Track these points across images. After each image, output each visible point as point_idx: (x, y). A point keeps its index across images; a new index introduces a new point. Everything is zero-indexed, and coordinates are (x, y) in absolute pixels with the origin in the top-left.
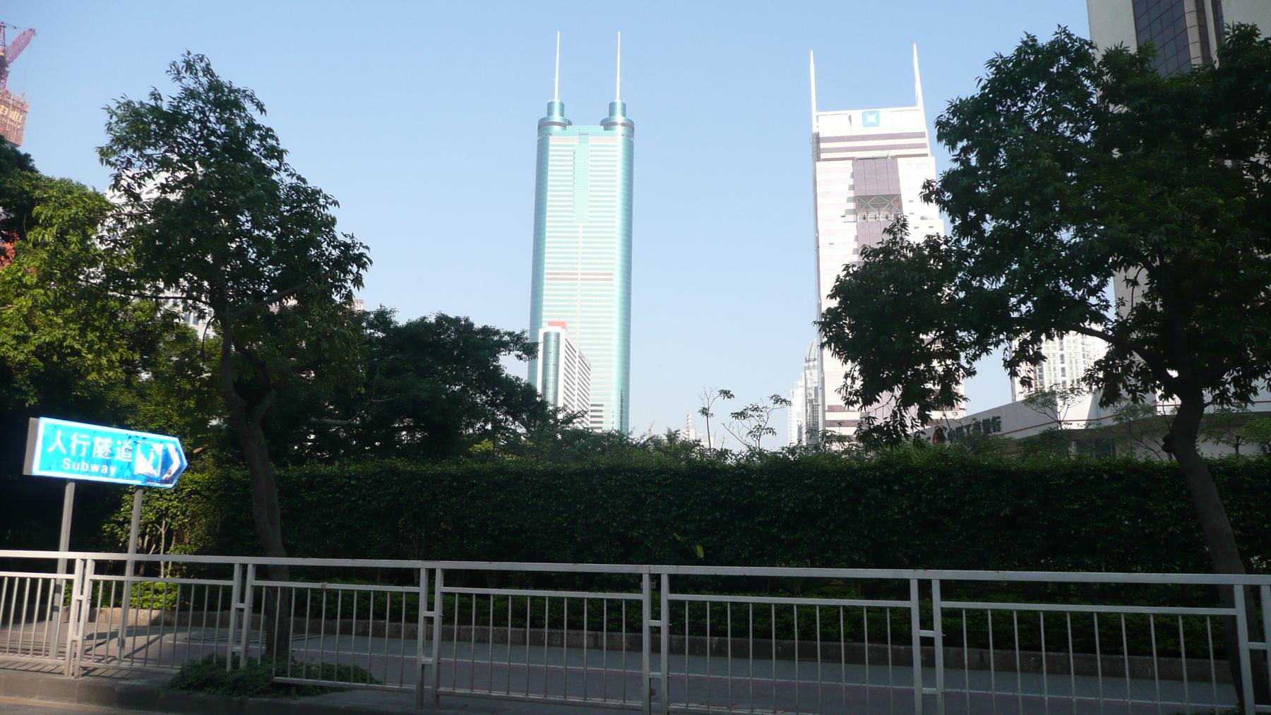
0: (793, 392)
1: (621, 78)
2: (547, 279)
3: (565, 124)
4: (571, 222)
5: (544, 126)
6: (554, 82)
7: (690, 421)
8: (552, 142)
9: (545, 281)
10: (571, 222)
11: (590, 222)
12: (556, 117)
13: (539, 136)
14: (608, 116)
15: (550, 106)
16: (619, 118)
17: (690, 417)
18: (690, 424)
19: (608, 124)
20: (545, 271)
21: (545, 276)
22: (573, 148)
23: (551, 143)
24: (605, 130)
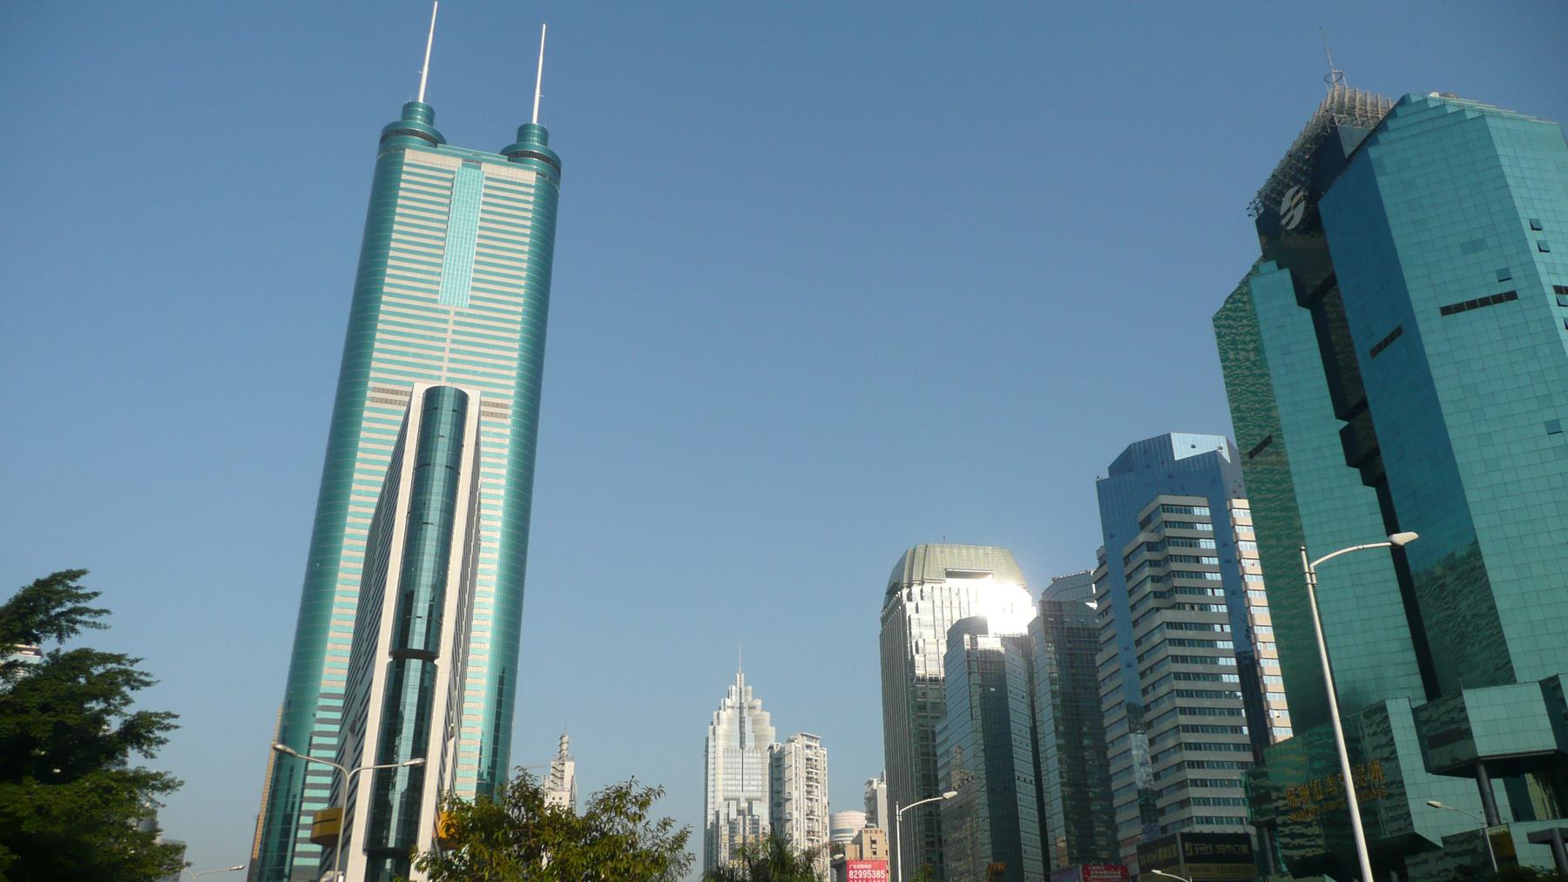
0: (718, 714)
1: (541, 94)
2: (373, 399)
3: (434, 140)
4: (435, 301)
5: (393, 138)
6: (421, 76)
7: (565, 746)
8: (410, 156)
9: (368, 404)
10: (435, 301)
11: (471, 306)
12: (419, 122)
14: (514, 141)
15: (409, 109)
16: (535, 144)
17: (565, 740)
18: (565, 752)
19: (515, 154)
20: (371, 384)
21: (369, 394)
22: (450, 176)
23: (406, 161)
24: (509, 160)
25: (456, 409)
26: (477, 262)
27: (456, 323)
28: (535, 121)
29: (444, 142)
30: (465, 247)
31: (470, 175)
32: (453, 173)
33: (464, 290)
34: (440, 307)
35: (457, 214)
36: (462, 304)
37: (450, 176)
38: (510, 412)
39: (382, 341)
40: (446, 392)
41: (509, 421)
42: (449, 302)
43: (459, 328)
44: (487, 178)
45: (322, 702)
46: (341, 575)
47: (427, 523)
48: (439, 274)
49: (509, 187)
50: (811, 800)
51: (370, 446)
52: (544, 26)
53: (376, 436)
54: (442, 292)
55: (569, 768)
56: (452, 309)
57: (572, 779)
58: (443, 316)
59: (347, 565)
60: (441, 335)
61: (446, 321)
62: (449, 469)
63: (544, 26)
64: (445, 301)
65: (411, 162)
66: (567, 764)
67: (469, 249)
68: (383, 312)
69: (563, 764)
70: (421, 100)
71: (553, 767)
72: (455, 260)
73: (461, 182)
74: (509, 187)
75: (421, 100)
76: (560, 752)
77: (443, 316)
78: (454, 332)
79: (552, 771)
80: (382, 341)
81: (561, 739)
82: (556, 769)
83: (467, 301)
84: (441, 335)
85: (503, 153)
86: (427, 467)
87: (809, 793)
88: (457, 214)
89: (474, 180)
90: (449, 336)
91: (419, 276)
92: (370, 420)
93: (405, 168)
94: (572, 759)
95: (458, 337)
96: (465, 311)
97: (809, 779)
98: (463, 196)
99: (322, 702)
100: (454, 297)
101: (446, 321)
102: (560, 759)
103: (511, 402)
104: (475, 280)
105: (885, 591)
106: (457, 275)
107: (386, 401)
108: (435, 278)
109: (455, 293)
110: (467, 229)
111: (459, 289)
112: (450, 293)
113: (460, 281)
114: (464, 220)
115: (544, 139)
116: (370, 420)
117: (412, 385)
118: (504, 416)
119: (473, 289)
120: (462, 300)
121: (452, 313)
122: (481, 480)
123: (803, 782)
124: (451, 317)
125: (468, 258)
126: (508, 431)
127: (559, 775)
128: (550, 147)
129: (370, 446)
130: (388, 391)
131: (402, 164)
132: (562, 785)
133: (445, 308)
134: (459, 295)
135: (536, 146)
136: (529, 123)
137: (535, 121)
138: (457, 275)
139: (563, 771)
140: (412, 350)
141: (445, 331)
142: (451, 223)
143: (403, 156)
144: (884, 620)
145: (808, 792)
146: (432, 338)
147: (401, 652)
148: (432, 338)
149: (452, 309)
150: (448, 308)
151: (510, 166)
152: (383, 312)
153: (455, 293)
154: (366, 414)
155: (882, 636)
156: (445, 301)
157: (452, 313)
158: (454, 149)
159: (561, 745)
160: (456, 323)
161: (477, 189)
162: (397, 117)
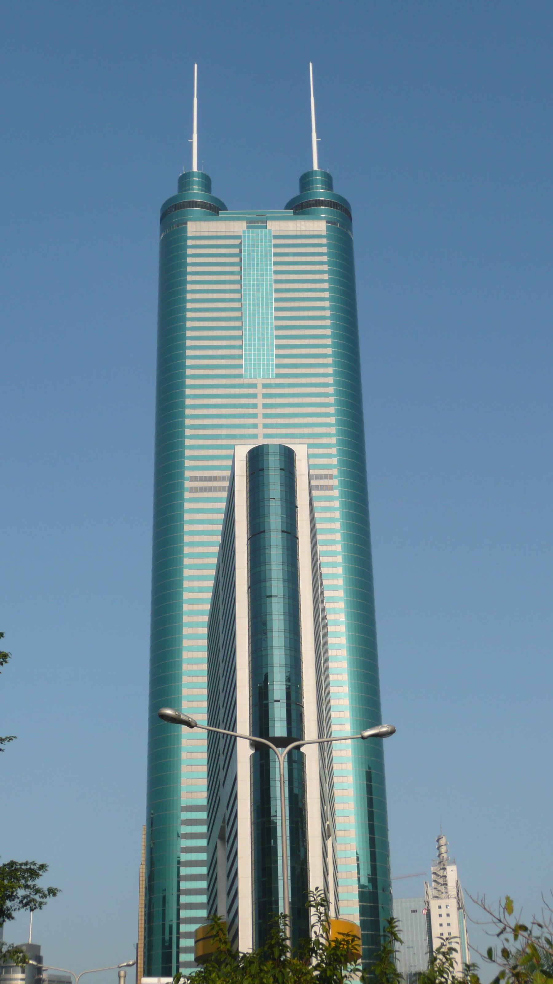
1: (318, 137)
2: (192, 490)
4: (240, 376)
6: (191, 144)
7: (443, 849)
9: (187, 495)
10: (240, 376)
11: (279, 376)
13: (162, 229)
17: (443, 841)
18: (445, 855)
20: (187, 474)
22: (236, 242)
23: (189, 234)
24: (295, 213)
25: (283, 468)
26: (278, 328)
27: (265, 396)
28: (316, 167)
29: (224, 208)
30: (263, 314)
31: (257, 235)
32: (239, 237)
33: (268, 359)
34: (246, 382)
35: (249, 281)
36: (268, 375)
37: (236, 242)
38: (335, 482)
39: (193, 427)
40: (271, 450)
41: (336, 493)
42: (255, 375)
43: (269, 401)
44: (275, 237)
45: (185, 816)
46: (185, 680)
47: (271, 596)
48: (240, 347)
49: (299, 241)
51: (196, 539)
52: (311, 65)
53: (200, 528)
54: (246, 366)
55: (452, 873)
56: (260, 382)
57: (457, 884)
58: (251, 391)
59: (190, 667)
60: (251, 411)
61: (254, 396)
62: (285, 534)
63: (311, 65)
64: (250, 374)
65: (194, 234)
66: (449, 868)
67: (267, 315)
68: (190, 397)
69: (444, 869)
70: (195, 169)
71: (434, 873)
72: (254, 329)
73: (249, 245)
74: (299, 241)
75: (195, 169)
76: (439, 856)
77: (251, 391)
78: (265, 406)
79: (433, 877)
80: (193, 427)
81: (438, 841)
82: (438, 875)
83: (273, 371)
84: (251, 411)
85: (288, 207)
86: (262, 535)
88: (249, 281)
89: (261, 241)
90: (260, 411)
91: (220, 352)
92: (192, 511)
93: (189, 242)
94: (453, 862)
95: (269, 411)
96: (273, 381)
98: (253, 260)
99: (185, 816)
100: (259, 369)
101: (254, 396)
102: (440, 863)
103: (335, 472)
104: (278, 347)
106: (259, 344)
107: (205, 489)
108: (236, 352)
109: (259, 364)
110: (262, 294)
111: (264, 360)
112: (255, 365)
113: (263, 350)
114: (258, 285)
116: (192, 511)
117: (232, 447)
118: (331, 488)
119: (278, 356)
120: (268, 370)
121: (260, 387)
122: (320, 548)
124: (260, 391)
125: (267, 324)
126: (336, 504)
127: (441, 881)
128: (336, 191)
129: (196, 539)
130: (206, 479)
131: (186, 238)
132: (447, 892)
133: (250, 382)
134: (264, 365)
135: (322, 194)
136: (310, 170)
137: (316, 167)
138: (259, 344)
139: (445, 877)
140: (224, 432)
141: (255, 406)
142: (245, 290)
143: (185, 230)
146: (242, 416)
148: (242, 416)
149: (260, 382)
150: (254, 382)
151: (296, 219)
152: (190, 397)
153: (259, 364)
154: (187, 506)
156: (250, 374)
157: (260, 387)
158: (234, 213)
159: (439, 848)
160: (265, 396)
161: (266, 250)
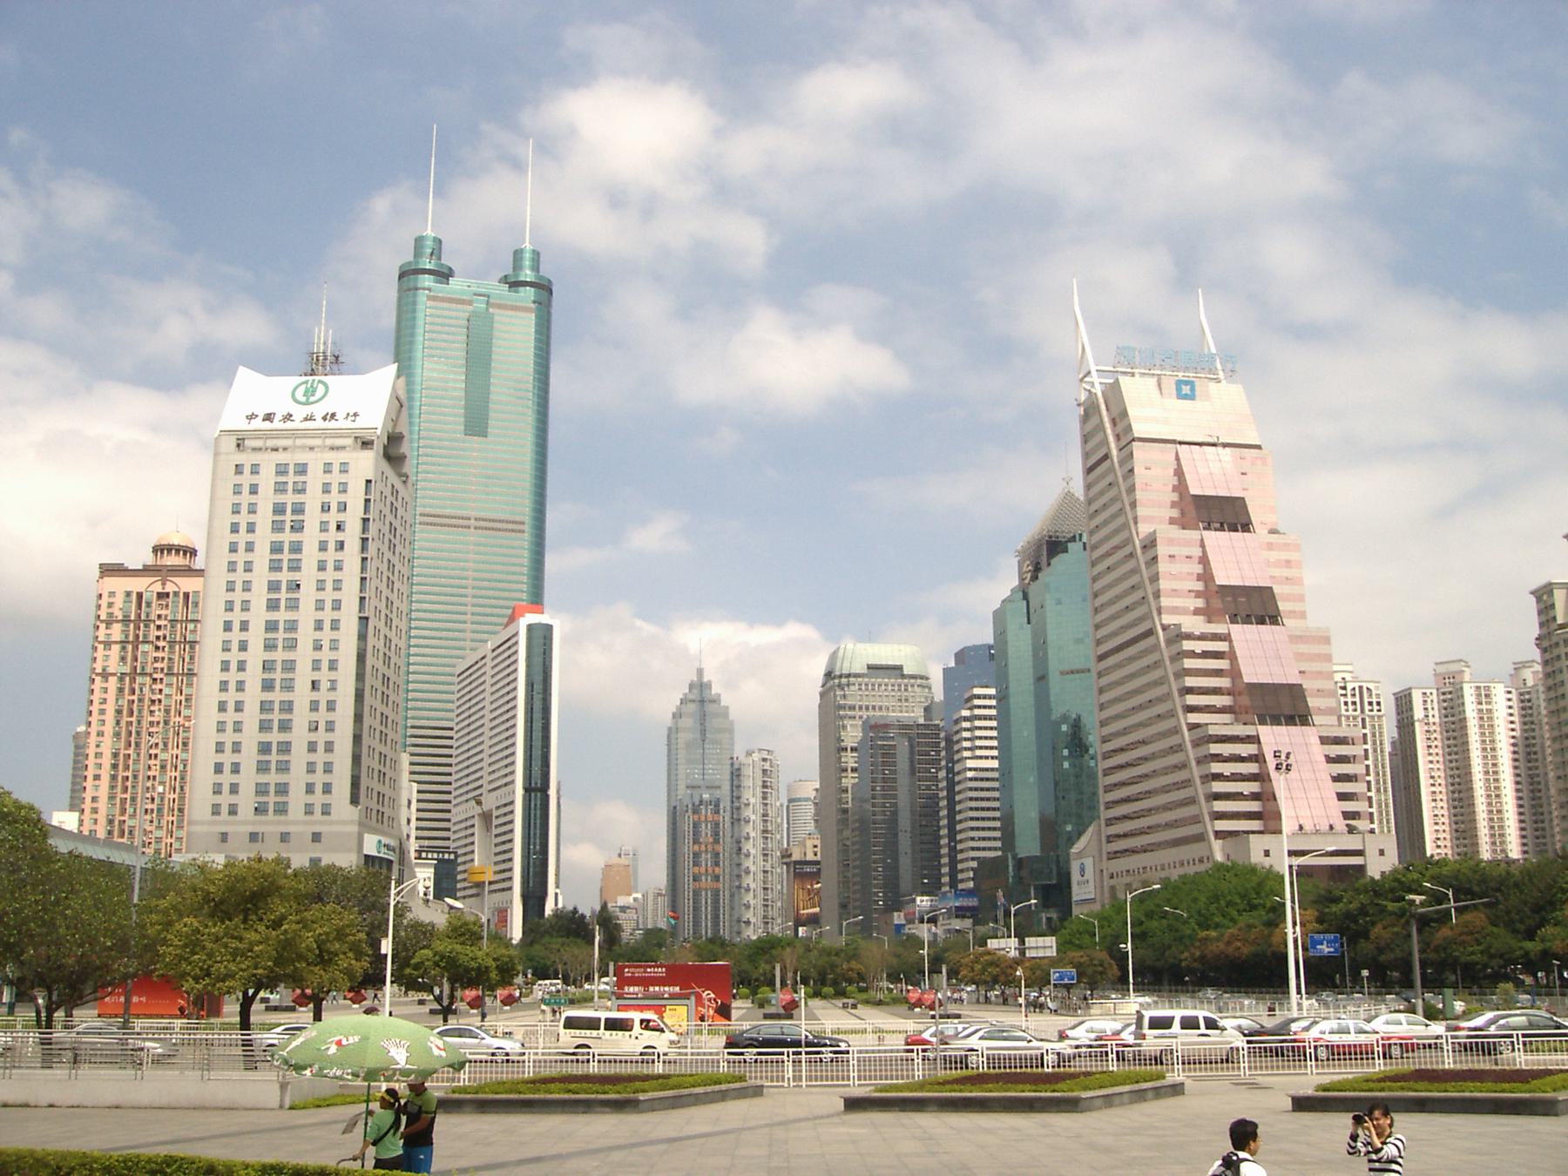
41: (526, 536)
50: (766, 805)
87: (764, 798)
97: (765, 786)
105: (823, 673)
115: (536, 267)
123: (759, 790)
144: (822, 695)
145: (763, 793)
147: (528, 790)
155: (820, 706)
162: (411, 258)
